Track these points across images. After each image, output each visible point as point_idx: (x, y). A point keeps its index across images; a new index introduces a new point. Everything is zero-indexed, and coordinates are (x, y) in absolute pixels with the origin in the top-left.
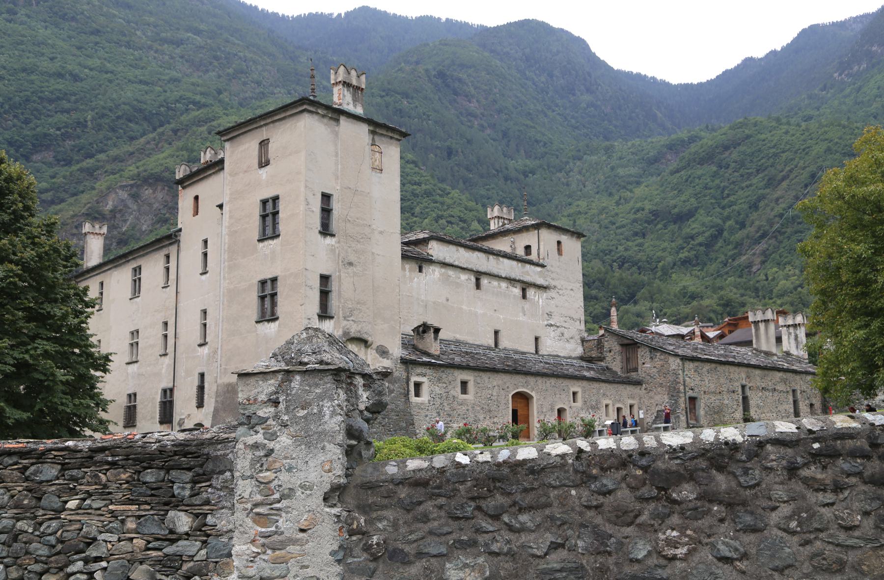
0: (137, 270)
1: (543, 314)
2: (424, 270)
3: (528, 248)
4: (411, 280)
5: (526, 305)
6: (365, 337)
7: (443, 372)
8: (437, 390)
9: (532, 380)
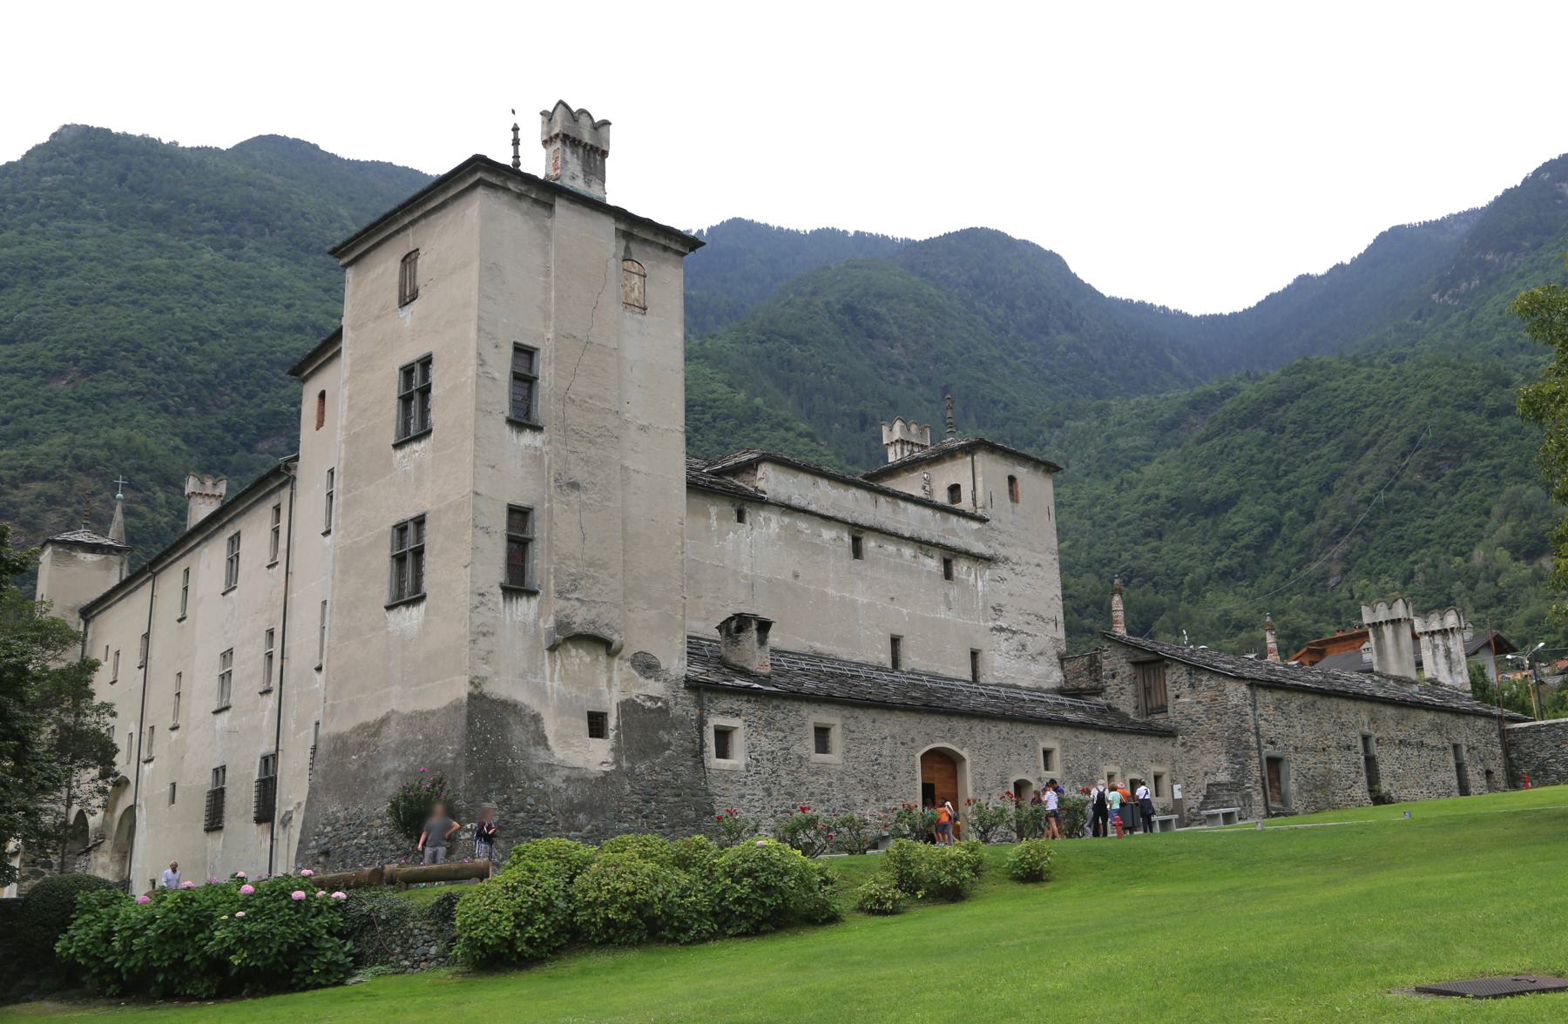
0: (235, 540)
1: (984, 608)
2: (747, 518)
3: (954, 490)
4: (722, 536)
5: (954, 592)
6: (606, 633)
7: (777, 707)
8: (765, 744)
9: (960, 725)
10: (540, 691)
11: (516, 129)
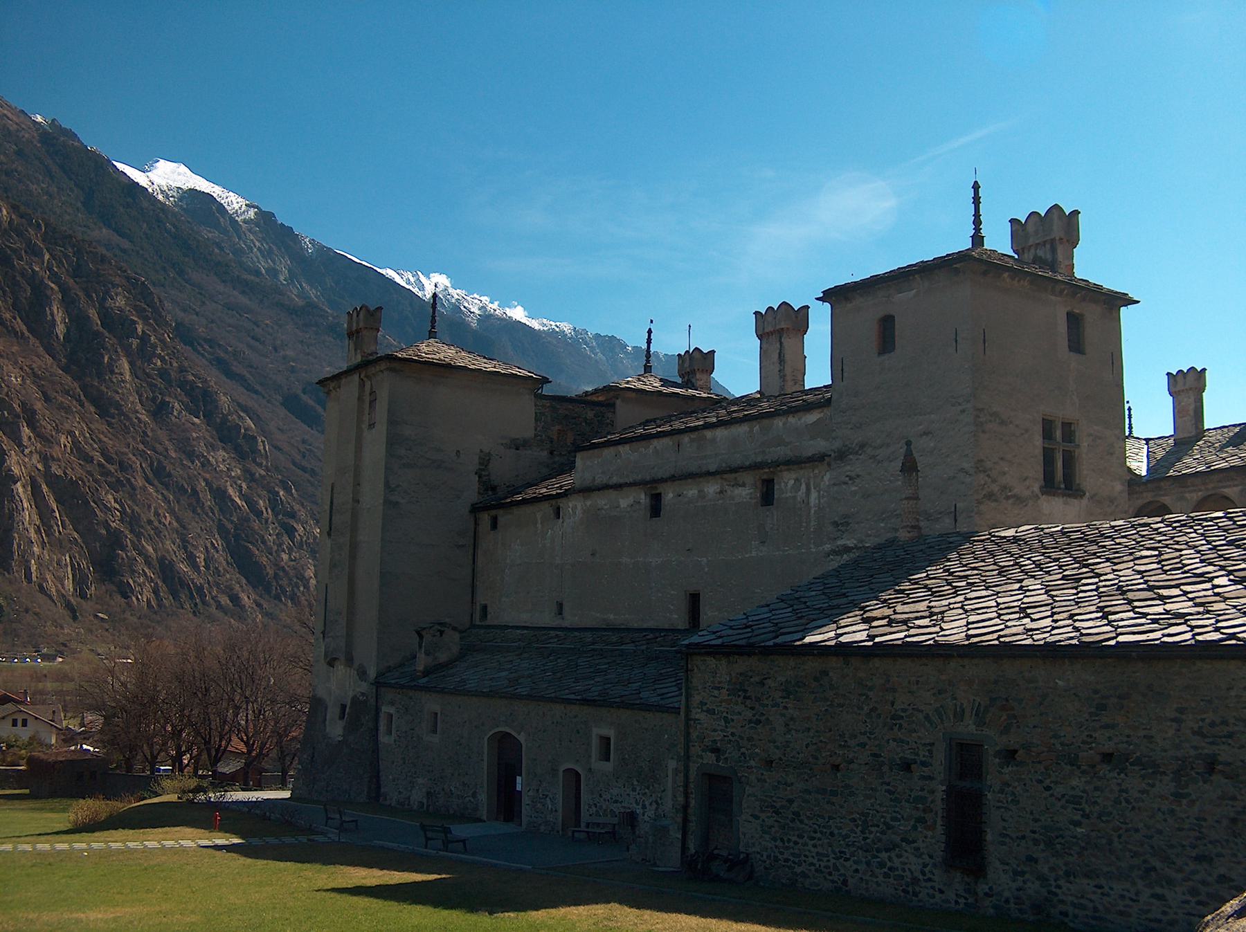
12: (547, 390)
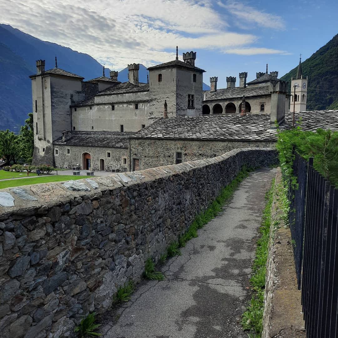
5: (137, 112)
10: (40, 146)
11: (56, 58)
12: (84, 80)
